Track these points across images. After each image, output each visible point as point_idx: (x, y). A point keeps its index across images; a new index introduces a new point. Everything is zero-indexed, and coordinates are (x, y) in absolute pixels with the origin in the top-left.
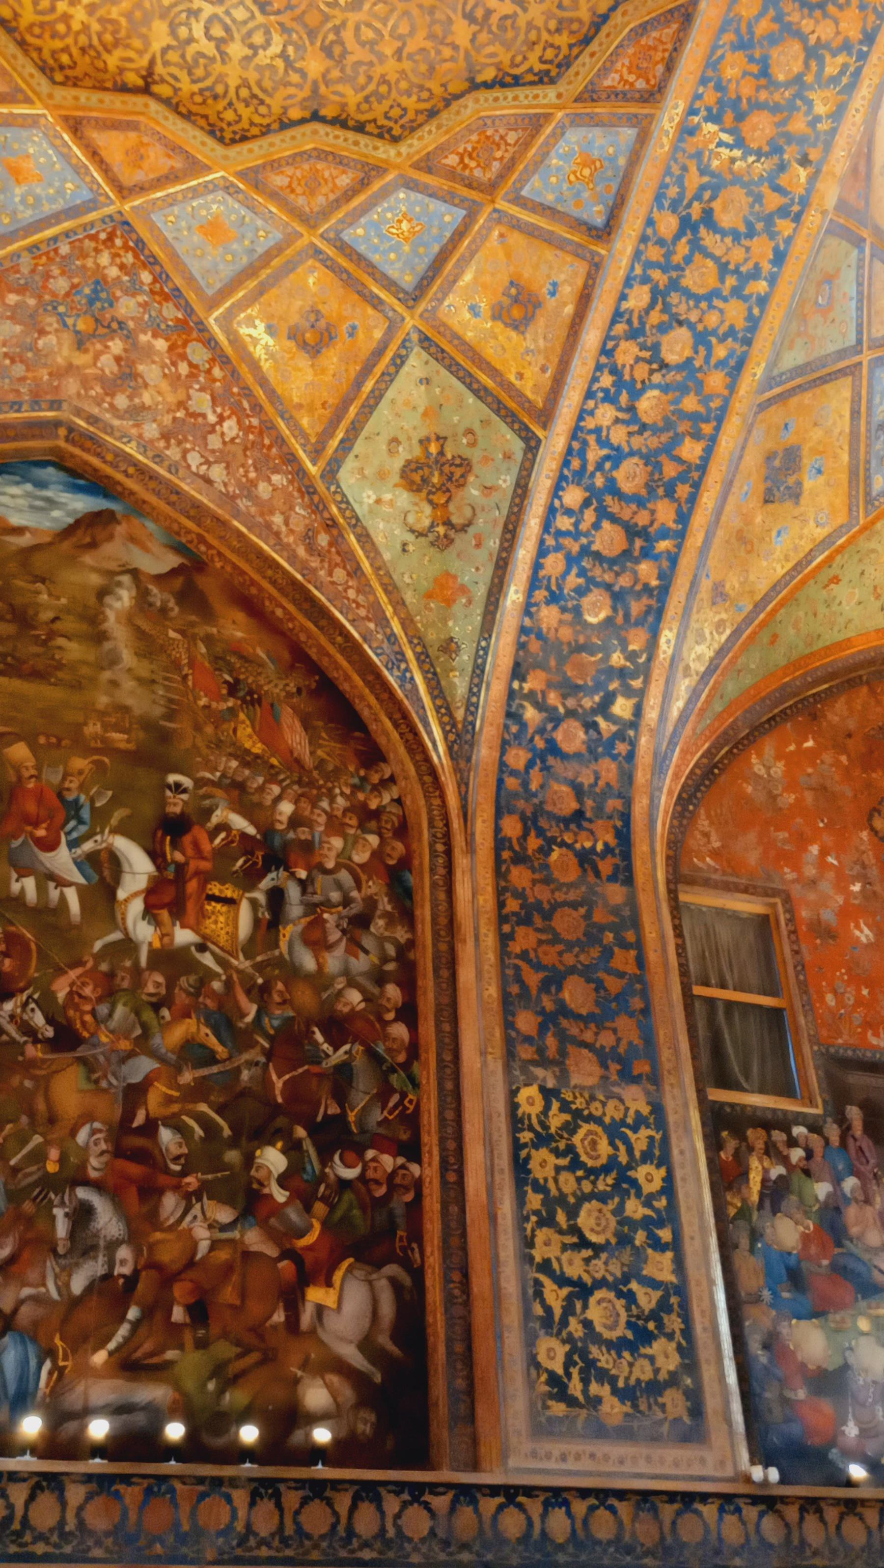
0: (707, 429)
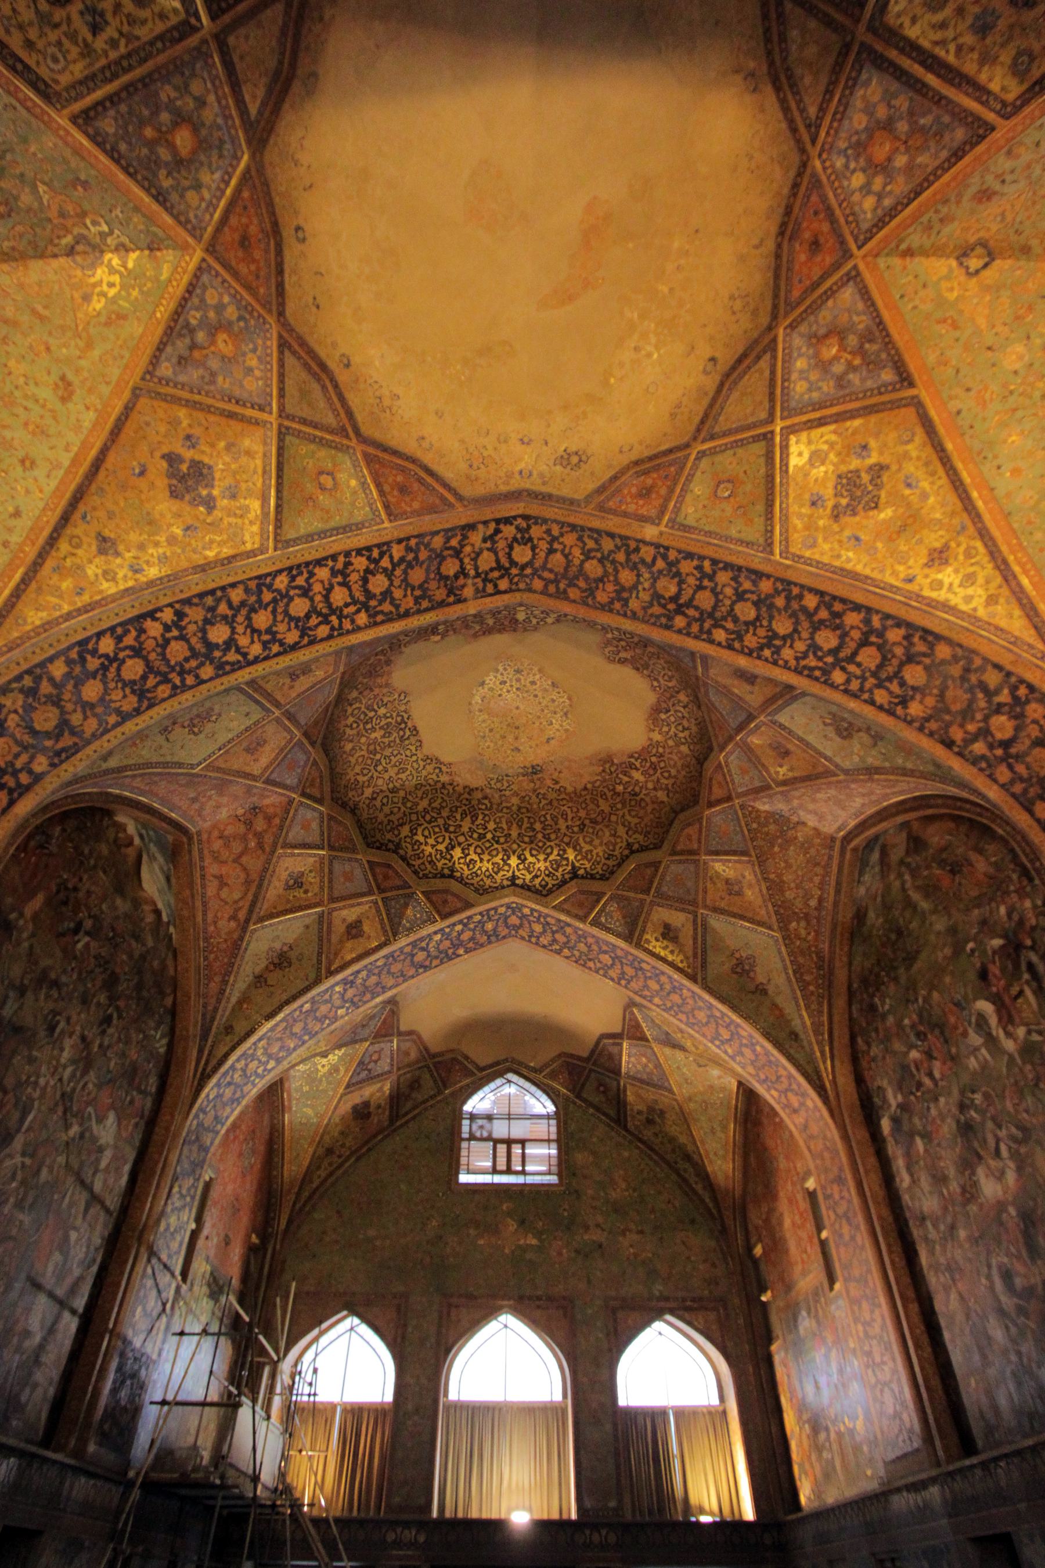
0: (796, 591)
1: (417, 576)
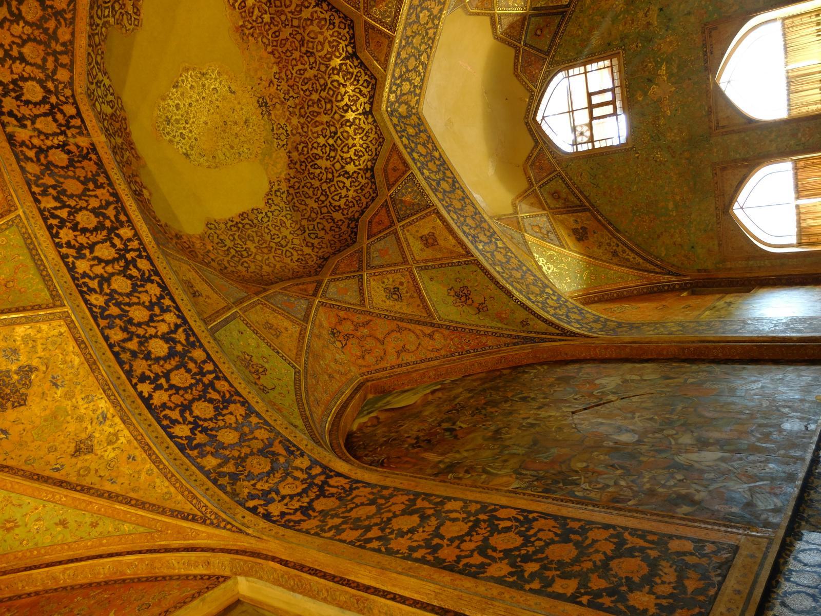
1: (73, 186)
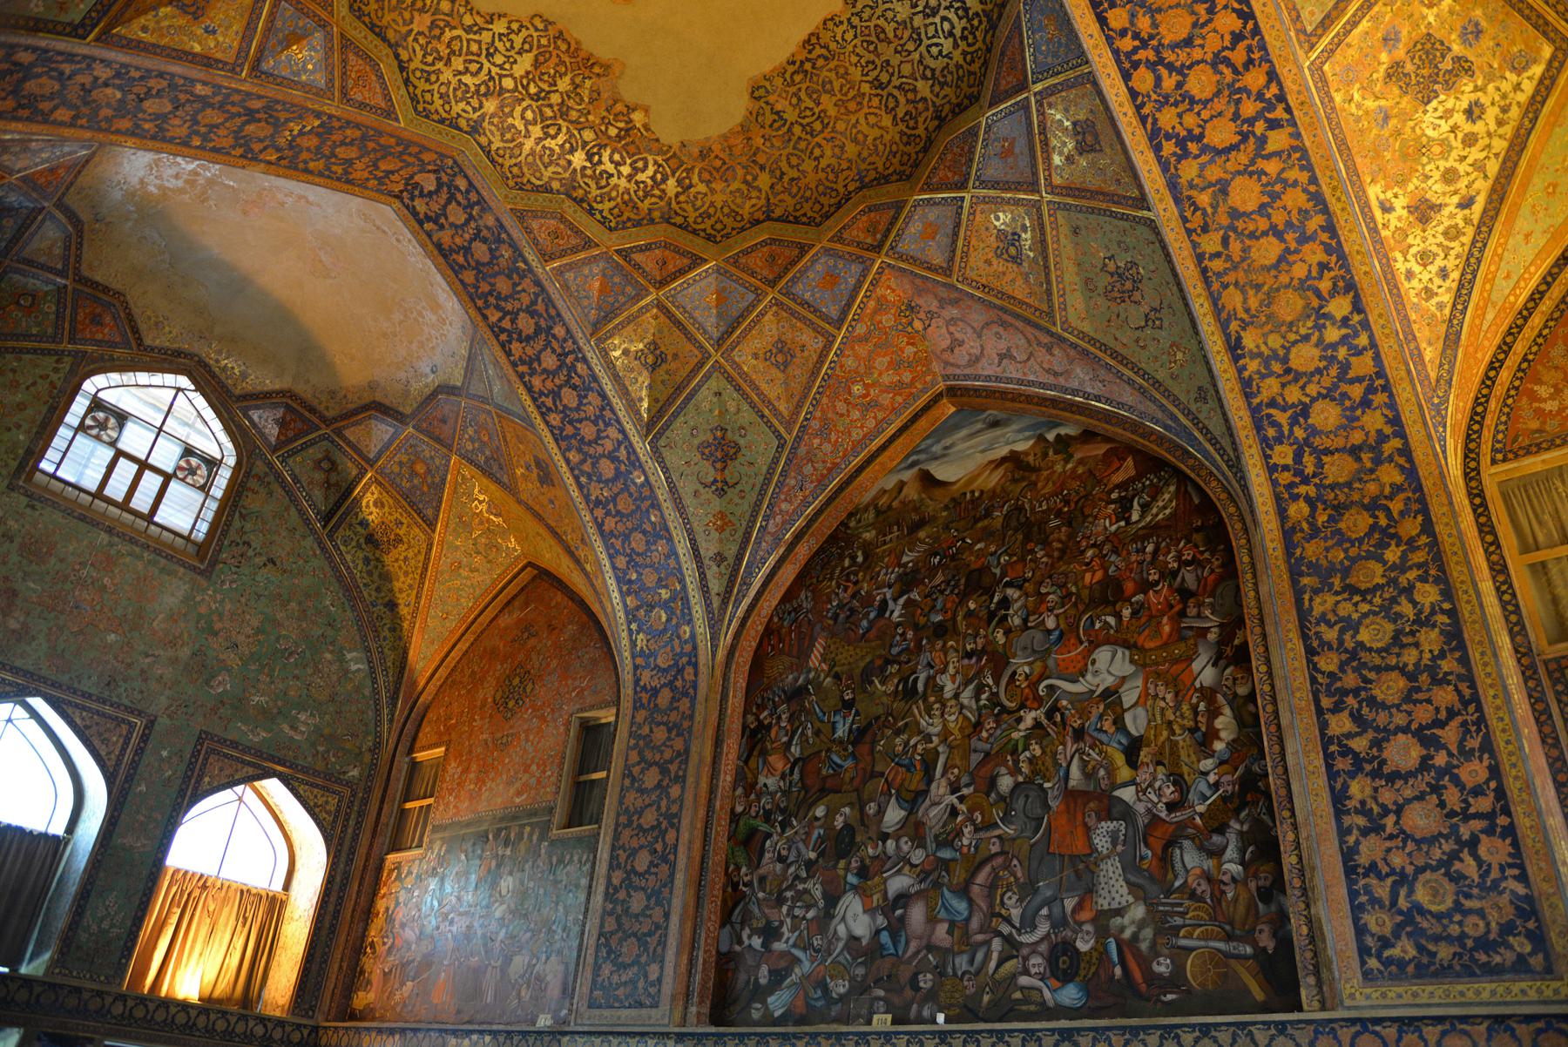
1: (503, 285)
